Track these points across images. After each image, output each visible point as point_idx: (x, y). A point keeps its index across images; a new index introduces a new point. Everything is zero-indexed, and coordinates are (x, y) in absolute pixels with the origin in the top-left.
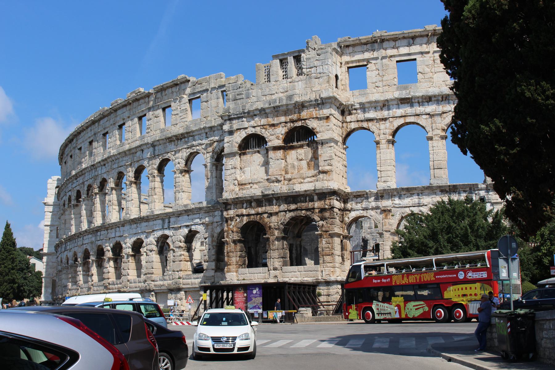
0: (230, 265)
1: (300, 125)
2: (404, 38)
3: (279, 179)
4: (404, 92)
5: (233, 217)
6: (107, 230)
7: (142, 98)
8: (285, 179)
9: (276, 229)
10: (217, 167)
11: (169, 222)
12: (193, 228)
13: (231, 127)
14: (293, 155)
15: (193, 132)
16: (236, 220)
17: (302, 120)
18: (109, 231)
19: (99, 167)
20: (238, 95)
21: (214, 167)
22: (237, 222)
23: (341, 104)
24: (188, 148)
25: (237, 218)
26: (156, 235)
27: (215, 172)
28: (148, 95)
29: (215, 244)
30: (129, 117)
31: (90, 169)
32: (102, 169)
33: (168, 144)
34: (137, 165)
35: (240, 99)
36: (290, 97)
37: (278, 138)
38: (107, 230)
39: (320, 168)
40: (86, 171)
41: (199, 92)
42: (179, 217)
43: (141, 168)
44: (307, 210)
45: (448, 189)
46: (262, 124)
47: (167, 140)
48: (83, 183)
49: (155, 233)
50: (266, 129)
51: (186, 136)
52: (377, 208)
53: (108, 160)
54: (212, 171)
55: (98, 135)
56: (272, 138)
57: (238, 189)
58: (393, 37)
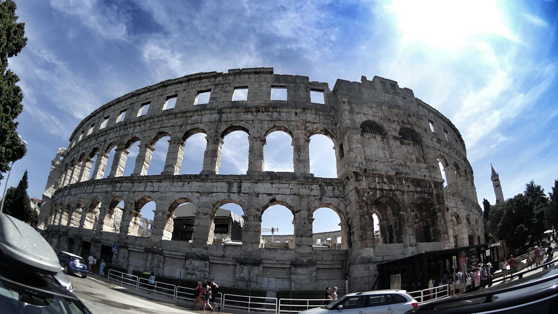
5: (366, 189)
6: (133, 183)
14: (404, 148)
16: (369, 193)
18: (135, 184)
19: (131, 127)
22: (370, 194)
24: (271, 121)
30: (184, 90)
31: (118, 129)
33: (241, 114)
37: (395, 130)
38: (133, 183)
42: (256, 183)
43: (192, 132)
46: (380, 116)
47: (243, 110)
51: (271, 110)
53: (147, 121)
54: (305, 147)
55: (136, 104)
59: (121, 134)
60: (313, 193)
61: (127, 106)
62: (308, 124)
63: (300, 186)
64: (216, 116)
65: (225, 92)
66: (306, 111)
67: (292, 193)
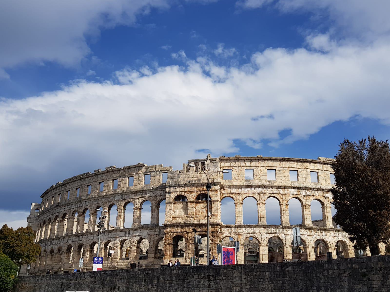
0: (166, 256)
1: (204, 193)
2: (248, 159)
3: (193, 216)
4: (248, 183)
5: (169, 233)
6: (88, 235)
7: (116, 171)
8: (195, 217)
9: (190, 239)
10: (157, 208)
11: (129, 233)
12: (143, 237)
13: (170, 191)
14: (199, 206)
15: (146, 190)
17: (204, 191)
18: (89, 236)
20: (174, 176)
21: (156, 208)
23: (221, 185)
24: (142, 198)
25: (171, 233)
26: (120, 239)
27: (156, 210)
28: (120, 170)
29: (155, 245)
32: (85, 203)
34: (110, 204)
35: (175, 178)
36: (199, 180)
37: (193, 198)
38: (88, 235)
39: (213, 213)
40: (73, 203)
41: (150, 172)
44: (205, 231)
45: (266, 227)
48: (70, 210)
49: (120, 238)
50: (187, 193)
51: (142, 192)
52: (235, 233)
56: (190, 197)
57: (172, 220)
58: (244, 158)
59: (78, 206)
60: (156, 233)
61: (79, 186)
62: (158, 197)
63: (151, 231)
64: (120, 196)
65: (124, 181)
66: (157, 190)
67: (148, 234)
